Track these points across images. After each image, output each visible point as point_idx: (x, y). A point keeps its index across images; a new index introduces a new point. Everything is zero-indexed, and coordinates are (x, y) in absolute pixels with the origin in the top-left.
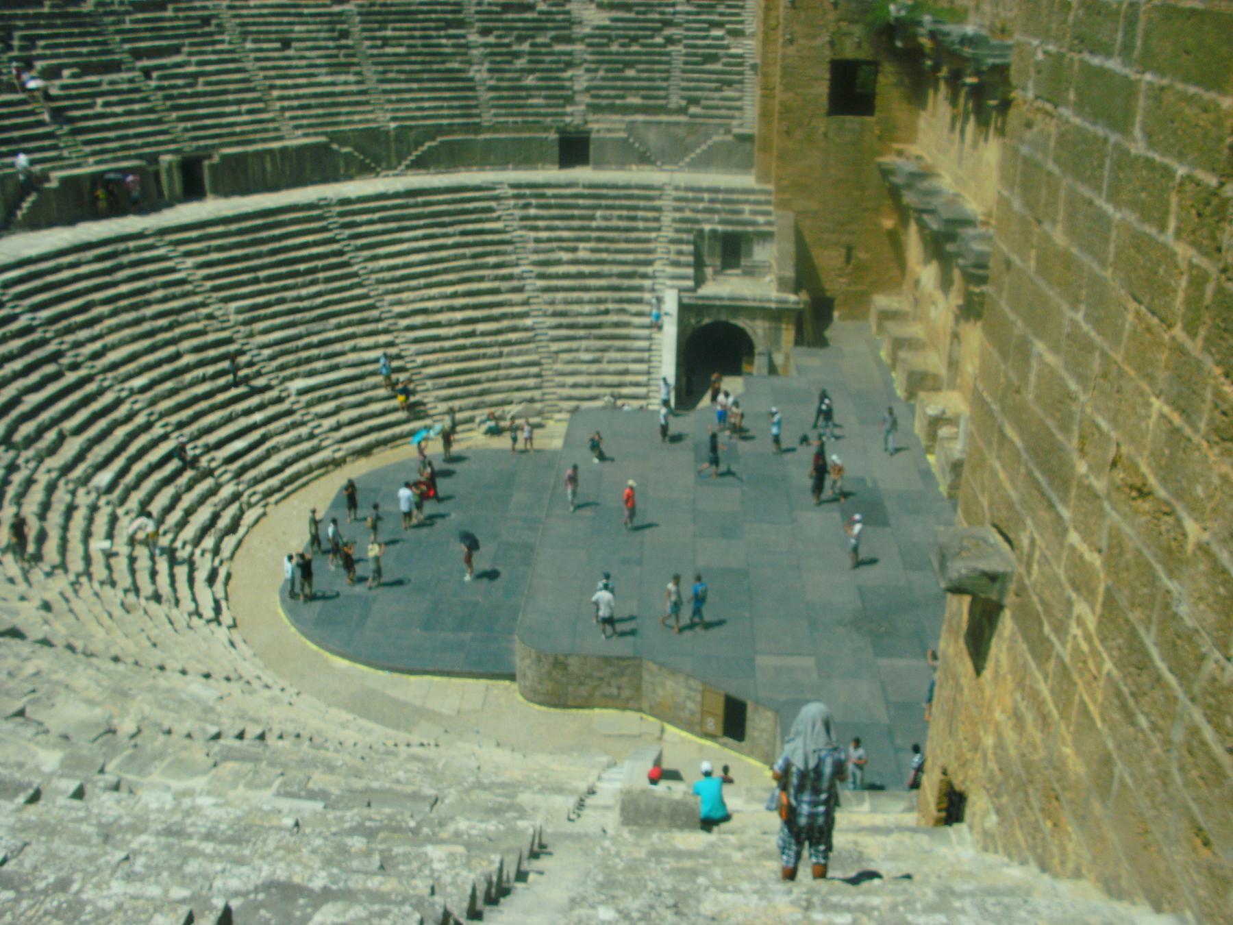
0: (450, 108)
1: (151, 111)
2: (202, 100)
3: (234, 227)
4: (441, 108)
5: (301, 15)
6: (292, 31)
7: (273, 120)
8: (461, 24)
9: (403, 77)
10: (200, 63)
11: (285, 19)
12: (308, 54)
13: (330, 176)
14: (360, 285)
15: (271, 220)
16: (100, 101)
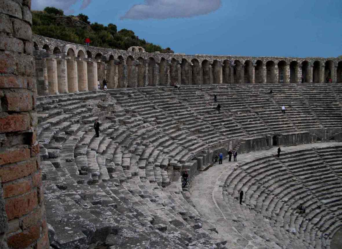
2: (273, 120)
3: (294, 155)
4: (338, 124)
5: (292, 99)
6: (291, 103)
8: (336, 101)
10: (270, 111)
12: (297, 109)
13: (309, 141)
14: (331, 173)
15: (302, 153)
16: (249, 120)
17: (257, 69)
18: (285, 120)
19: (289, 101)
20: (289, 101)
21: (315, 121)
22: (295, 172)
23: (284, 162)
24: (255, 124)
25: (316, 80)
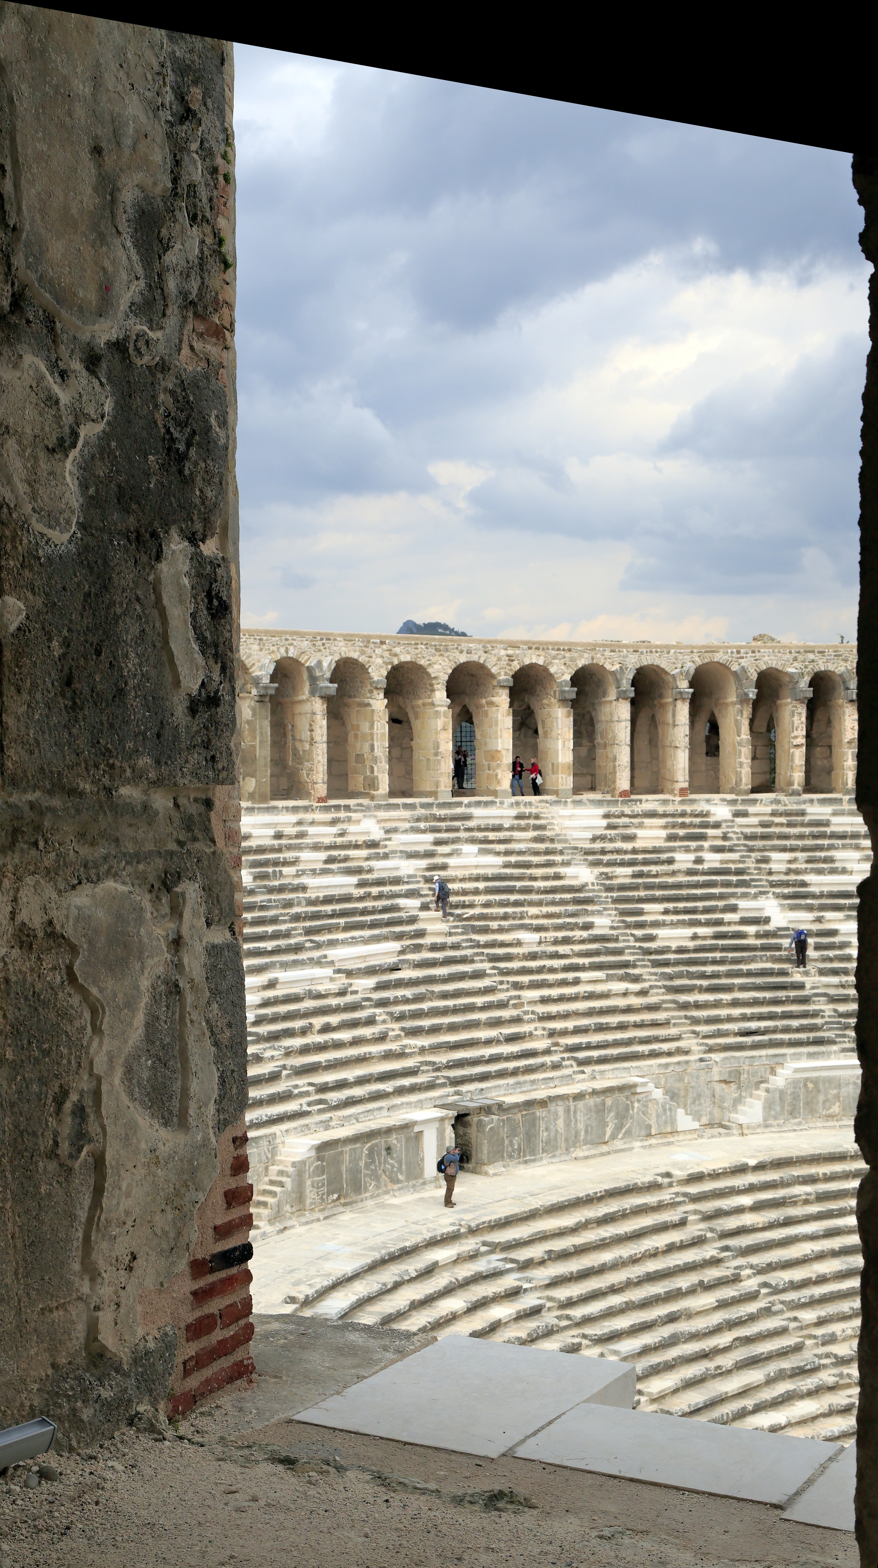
0: (787, 1030)
1: (382, 1038)
7: (547, 1052)
9: (705, 983)
11: (513, 897)
12: (562, 949)
14: (767, 1312)
16: (318, 1022)
17: (338, 709)
18: (506, 1014)
19: (517, 904)
20: (517, 904)
21: (661, 1016)
22: (588, 1320)
23: (527, 1265)
24: (356, 1042)
25: (648, 776)
